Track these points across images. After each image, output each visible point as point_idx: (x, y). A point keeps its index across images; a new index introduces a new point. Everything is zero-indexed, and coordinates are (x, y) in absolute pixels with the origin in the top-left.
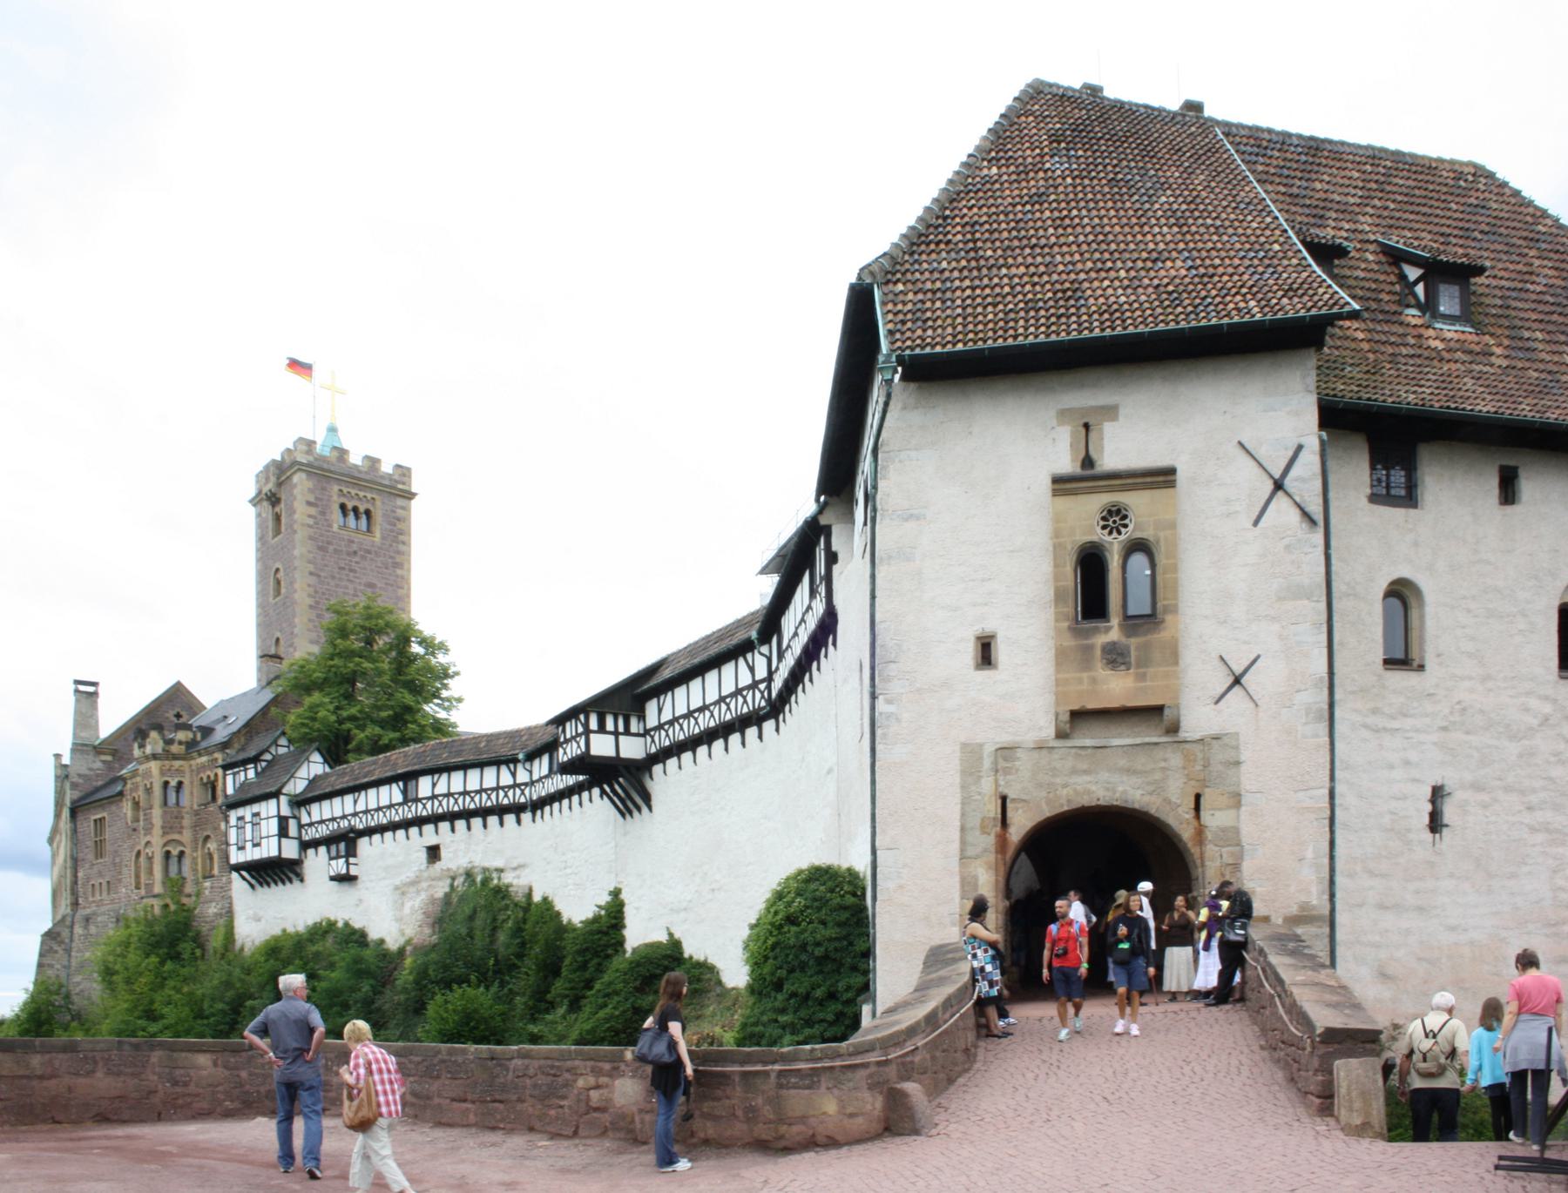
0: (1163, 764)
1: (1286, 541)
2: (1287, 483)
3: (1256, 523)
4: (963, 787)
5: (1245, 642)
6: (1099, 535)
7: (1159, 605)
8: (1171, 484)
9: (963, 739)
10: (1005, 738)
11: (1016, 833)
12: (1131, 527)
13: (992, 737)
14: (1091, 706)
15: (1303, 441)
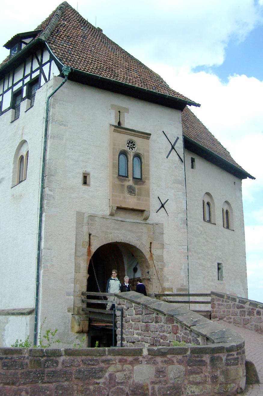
0: (141, 231)
1: (175, 165)
2: (175, 147)
3: (167, 157)
4: (77, 228)
5: (164, 194)
6: (126, 148)
7: (143, 176)
8: (148, 138)
9: (77, 210)
10: (92, 212)
11: (94, 249)
12: (136, 148)
13: (87, 210)
14: (123, 206)
15: (179, 136)
